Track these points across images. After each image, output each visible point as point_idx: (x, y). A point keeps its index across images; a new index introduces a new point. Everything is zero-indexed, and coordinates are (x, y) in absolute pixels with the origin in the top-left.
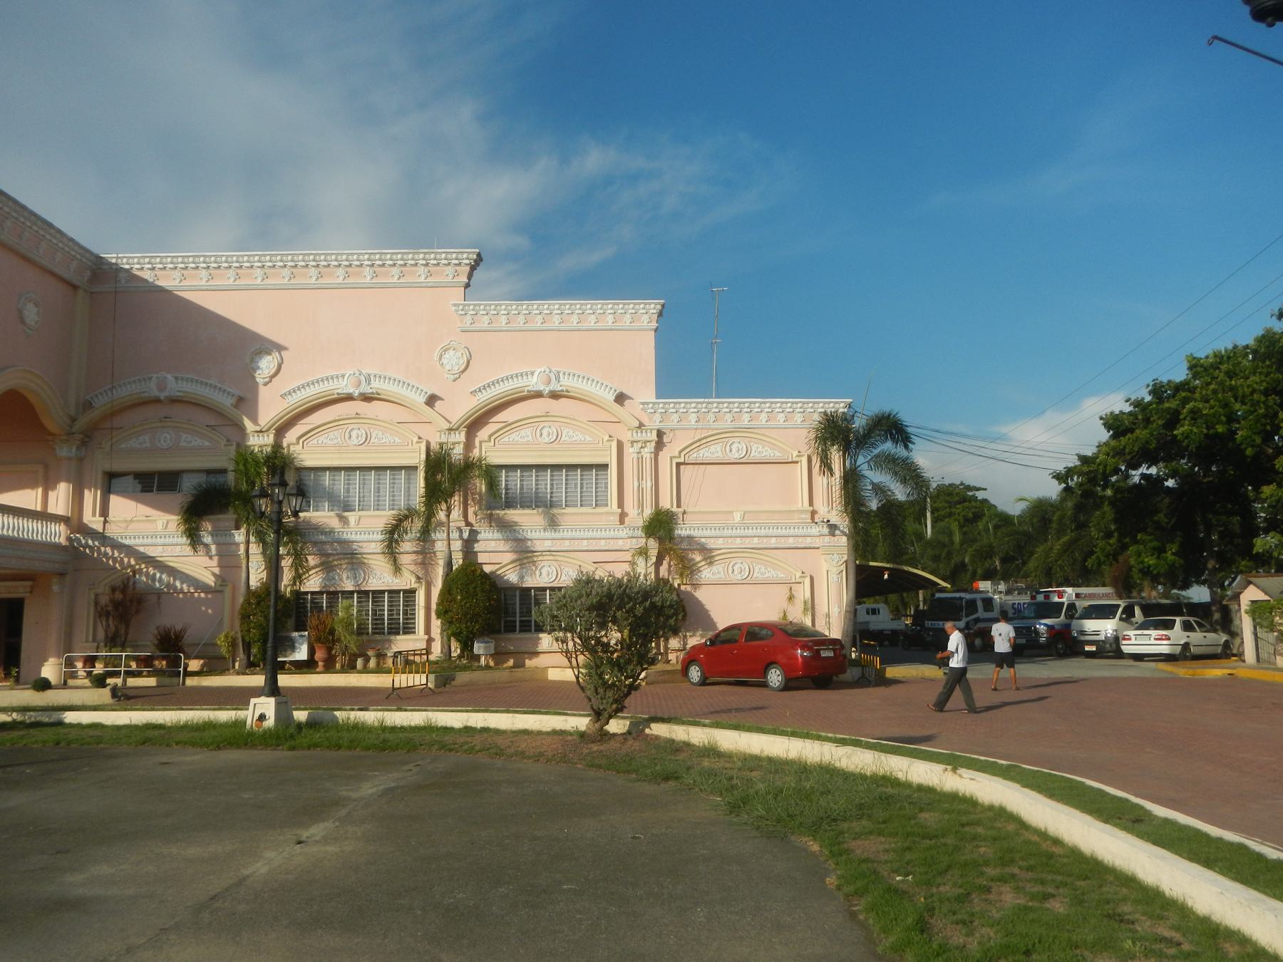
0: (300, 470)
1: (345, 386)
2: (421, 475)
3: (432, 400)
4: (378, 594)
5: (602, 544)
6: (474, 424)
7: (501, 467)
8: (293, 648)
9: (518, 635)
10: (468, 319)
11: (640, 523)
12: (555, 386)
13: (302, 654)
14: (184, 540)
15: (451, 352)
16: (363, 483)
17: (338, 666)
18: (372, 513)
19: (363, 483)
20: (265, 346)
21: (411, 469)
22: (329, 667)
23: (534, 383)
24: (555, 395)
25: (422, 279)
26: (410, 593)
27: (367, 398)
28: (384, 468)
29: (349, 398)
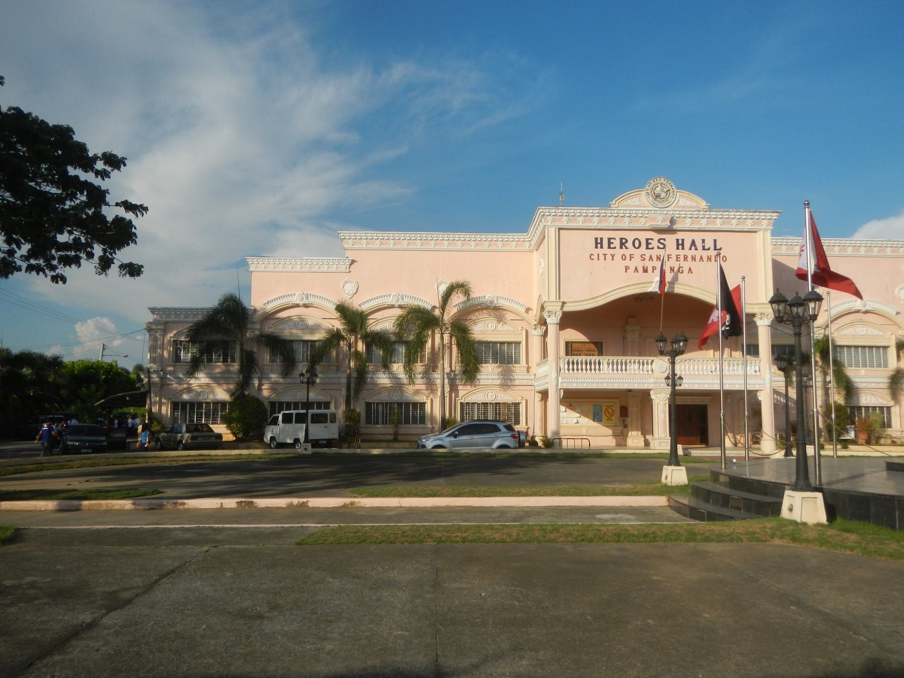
0: (835, 347)
2: (892, 352)
3: (898, 313)
4: (874, 408)
8: (847, 431)
9: (403, 426)
13: (852, 435)
14: (784, 379)
16: (864, 354)
17: (860, 441)
18: (868, 368)
19: (864, 354)
21: (885, 348)
22: (868, 442)
25: (889, 253)
26: (889, 408)
27: (866, 312)
28: (871, 347)
29: (858, 312)
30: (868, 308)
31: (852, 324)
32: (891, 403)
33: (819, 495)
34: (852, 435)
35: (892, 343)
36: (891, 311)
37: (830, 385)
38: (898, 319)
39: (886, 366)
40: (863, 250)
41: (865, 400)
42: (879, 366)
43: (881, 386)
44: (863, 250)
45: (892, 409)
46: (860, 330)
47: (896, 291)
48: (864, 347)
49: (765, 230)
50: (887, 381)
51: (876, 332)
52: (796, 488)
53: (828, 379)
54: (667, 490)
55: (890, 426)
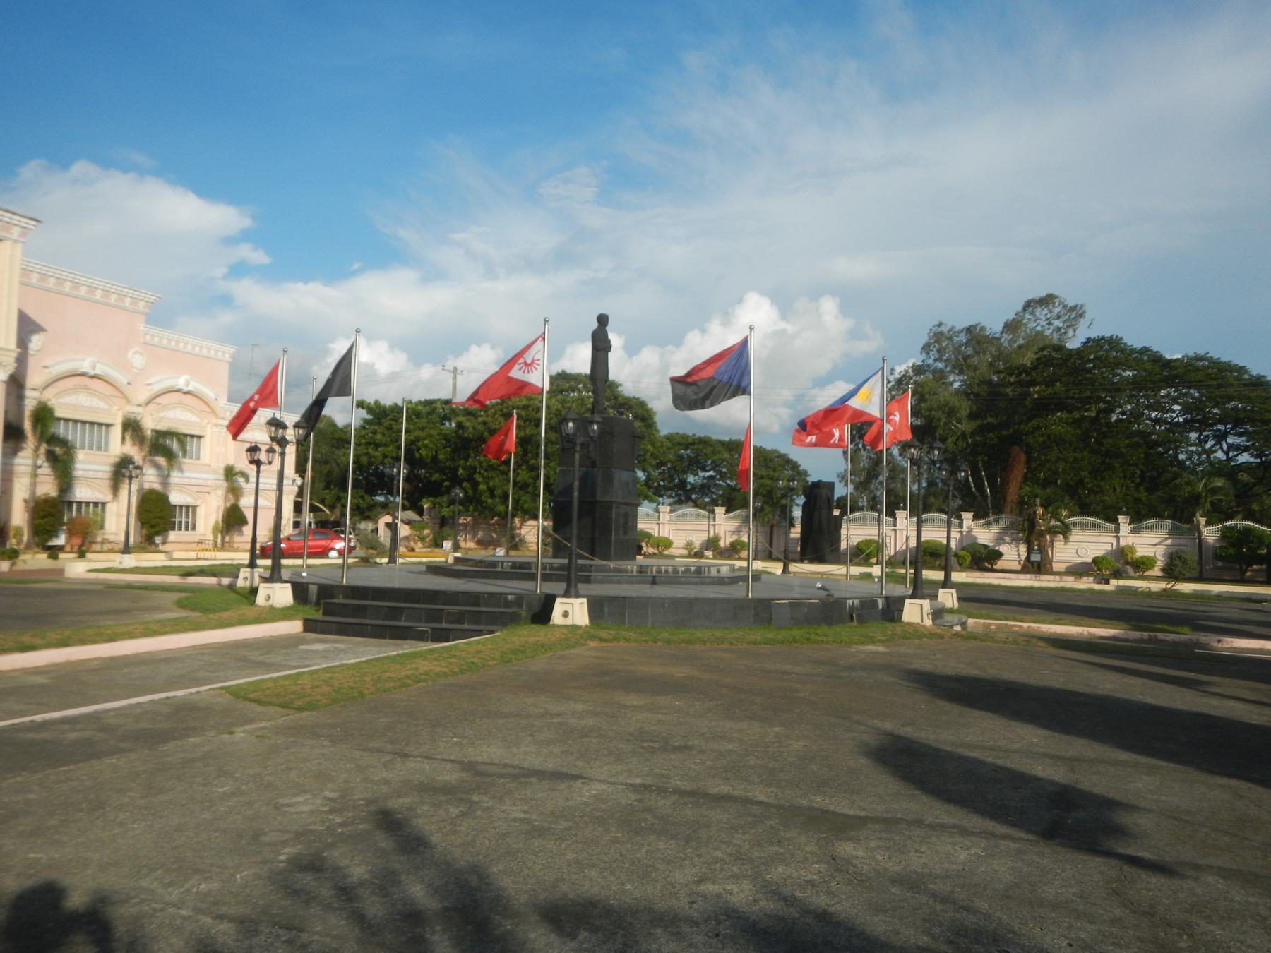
1: (86, 366)
2: (117, 432)
4: (88, 504)
5: (201, 482)
6: (149, 402)
7: (186, 435)
8: (57, 536)
10: (148, 337)
11: (222, 471)
12: (190, 388)
15: (138, 357)
16: (83, 431)
18: (86, 451)
19: (83, 431)
20: (38, 329)
21: (108, 426)
23: (181, 382)
24: (185, 393)
26: (104, 504)
29: (83, 374)
30: (97, 372)
31: (76, 390)
32: (109, 497)
33: (585, 600)
34: (61, 540)
35: (118, 422)
36: (120, 378)
37: (39, 471)
38: (127, 390)
39: (106, 450)
40: (98, 294)
41: (81, 493)
42: (99, 448)
43: (100, 475)
44: (98, 295)
45: (108, 506)
46: (84, 399)
47: (130, 353)
48: (84, 423)
49: (15, 241)
50: (108, 468)
51: (102, 405)
52: (566, 594)
53: (39, 463)
54: (275, 614)
55: (102, 527)
